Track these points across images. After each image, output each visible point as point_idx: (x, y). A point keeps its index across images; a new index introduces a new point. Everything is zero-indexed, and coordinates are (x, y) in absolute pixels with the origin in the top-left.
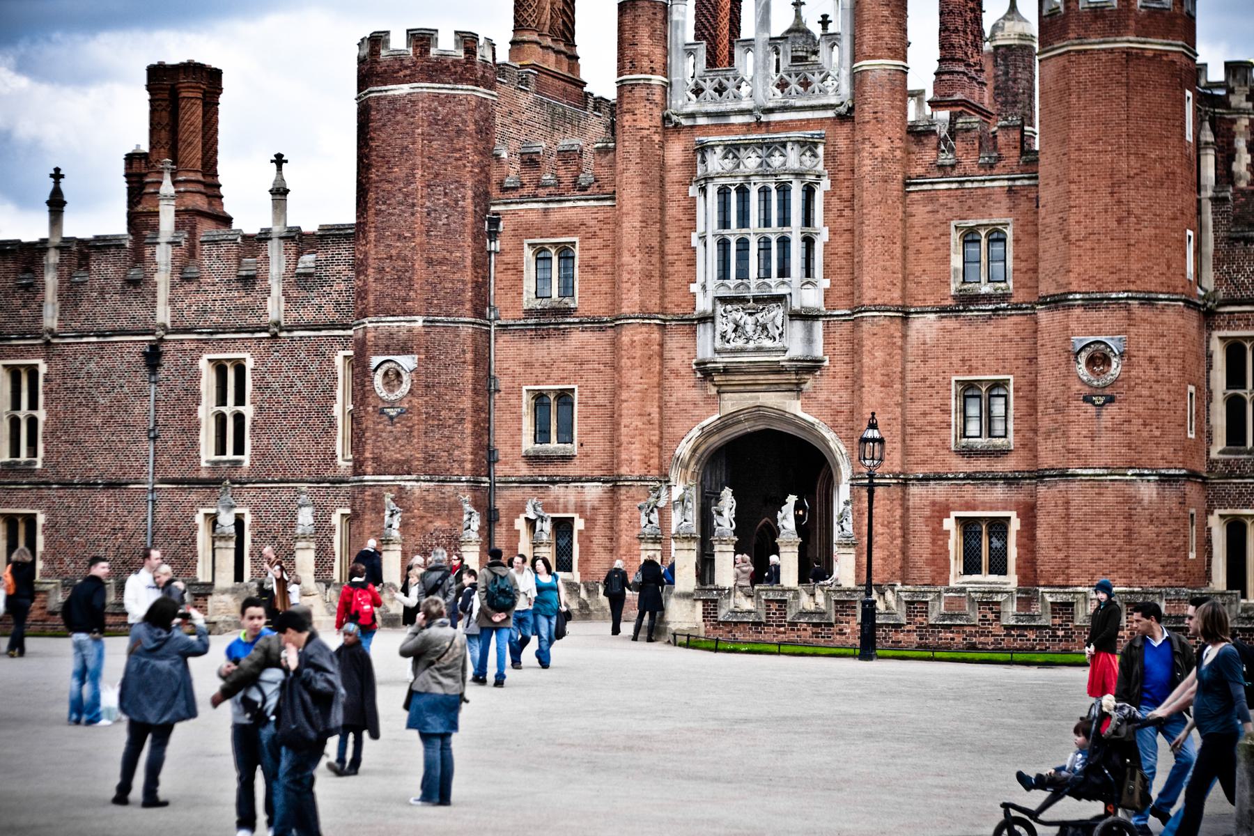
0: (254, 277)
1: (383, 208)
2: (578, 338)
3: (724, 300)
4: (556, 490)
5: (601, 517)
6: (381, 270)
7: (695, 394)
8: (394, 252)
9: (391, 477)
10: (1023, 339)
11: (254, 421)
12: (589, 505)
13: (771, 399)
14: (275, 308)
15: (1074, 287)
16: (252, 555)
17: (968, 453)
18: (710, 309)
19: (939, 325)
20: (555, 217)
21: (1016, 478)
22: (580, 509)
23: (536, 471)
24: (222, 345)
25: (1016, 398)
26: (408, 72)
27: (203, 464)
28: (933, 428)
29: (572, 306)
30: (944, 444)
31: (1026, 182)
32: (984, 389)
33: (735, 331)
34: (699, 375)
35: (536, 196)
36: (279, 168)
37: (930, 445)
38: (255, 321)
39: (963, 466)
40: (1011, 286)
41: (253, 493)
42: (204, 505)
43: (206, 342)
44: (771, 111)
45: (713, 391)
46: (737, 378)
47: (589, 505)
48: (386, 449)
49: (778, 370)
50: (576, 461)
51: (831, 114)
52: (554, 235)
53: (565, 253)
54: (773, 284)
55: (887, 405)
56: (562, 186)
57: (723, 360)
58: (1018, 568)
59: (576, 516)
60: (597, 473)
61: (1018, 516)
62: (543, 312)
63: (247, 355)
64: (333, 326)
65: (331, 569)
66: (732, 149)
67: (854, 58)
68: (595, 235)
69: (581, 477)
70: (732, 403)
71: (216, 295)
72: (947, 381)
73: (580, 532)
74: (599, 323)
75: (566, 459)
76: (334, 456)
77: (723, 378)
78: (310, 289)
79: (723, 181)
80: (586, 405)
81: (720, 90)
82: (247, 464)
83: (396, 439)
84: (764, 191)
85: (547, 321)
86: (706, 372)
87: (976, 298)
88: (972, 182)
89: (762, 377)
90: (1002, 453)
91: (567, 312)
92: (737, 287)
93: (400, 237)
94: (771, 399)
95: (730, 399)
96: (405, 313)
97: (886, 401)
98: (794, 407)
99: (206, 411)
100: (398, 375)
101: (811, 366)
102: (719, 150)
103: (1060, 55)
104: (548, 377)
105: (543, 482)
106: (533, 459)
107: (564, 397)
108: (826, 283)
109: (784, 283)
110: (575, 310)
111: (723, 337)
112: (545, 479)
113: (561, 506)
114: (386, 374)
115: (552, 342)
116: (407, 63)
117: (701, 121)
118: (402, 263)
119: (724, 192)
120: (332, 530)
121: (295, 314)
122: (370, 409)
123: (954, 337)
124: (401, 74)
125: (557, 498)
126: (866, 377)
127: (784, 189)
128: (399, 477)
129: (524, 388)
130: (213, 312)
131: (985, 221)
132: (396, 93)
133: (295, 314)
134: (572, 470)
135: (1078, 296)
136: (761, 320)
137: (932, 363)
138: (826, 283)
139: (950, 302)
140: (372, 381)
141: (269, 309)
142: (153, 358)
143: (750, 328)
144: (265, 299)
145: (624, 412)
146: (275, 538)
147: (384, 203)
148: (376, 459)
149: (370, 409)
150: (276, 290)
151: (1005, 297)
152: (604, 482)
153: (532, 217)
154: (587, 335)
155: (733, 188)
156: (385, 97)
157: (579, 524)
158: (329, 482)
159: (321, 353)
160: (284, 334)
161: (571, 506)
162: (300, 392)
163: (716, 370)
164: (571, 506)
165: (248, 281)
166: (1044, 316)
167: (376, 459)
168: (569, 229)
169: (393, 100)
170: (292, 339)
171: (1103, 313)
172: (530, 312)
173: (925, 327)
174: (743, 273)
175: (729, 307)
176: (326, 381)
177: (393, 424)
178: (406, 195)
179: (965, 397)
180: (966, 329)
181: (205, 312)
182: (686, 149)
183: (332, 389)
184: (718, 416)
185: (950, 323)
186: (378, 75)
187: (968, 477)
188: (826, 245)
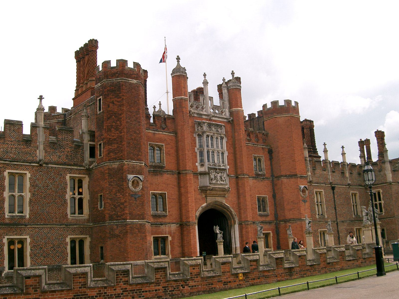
0: (30, 141)
1: (129, 121)
2: (166, 176)
3: (212, 169)
4: (163, 227)
5: (176, 236)
6: (129, 143)
8: (133, 138)
9: (137, 221)
11: (31, 200)
12: (172, 232)
13: (219, 199)
14: (40, 154)
15: (297, 173)
16: (31, 255)
17: (261, 216)
18: (207, 170)
19: (252, 181)
20: (157, 136)
21: (271, 222)
22: (170, 233)
23: (156, 220)
26: (136, 76)
27: (6, 217)
29: (164, 166)
30: (256, 212)
31: (265, 147)
34: (200, 191)
35: (150, 128)
36: (41, 101)
38: (31, 158)
41: (30, 229)
42: (7, 235)
43: (7, 165)
44: (213, 116)
45: (204, 196)
47: (172, 232)
48: (134, 210)
49: (224, 190)
50: (168, 217)
51: (225, 120)
52: (157, 142)
53: (160, 149)
54: (221, 166)
56: (157, 126)
57: (212, 186)
58: (273, 246)
59: (169, 236)
60: (174, 221)
61: (272, 232)
62: (155, 167)
63: (27, 172)
64: (65, 164)
65: (67, 260)
66: (210, 125)
67: (230, 108)
68: (169, 144)
69: (170, 222)
70: (210, 200)
73: (170, 241)
74: (172, 172)
75: (165, 216)
76: (66, 215)
78: (55, 149)
79: (208, 134)
80: (170, 199)
81: (197, 108)
82: (28, 216)
83: (138, 206)
85: (156, 170)
86: (204, 190)
88: (255, 144)
89: (219, 192)
90: (267, 216)
91: (162, 167)
93: (135, 132)
96: (138, 160)
98: (224, 201)
100: (138, 182)
102: (206, 124)
103: (287, 116)
104: (158, 189)
105: (159, 224)
106: (155, 216)
107: (163, 196)
108: (228, 167)
109: (223, 165)
110: (165, 167)
112: (159, 223)
113: (164, 233)
114: (133, 182)
115: (158, 177)
116: (135, 73)
117: (195, 115)
118: (136, 142)
120: (66, 244)
121: (49, 158)
122: (127, 194)
124: (133, 76)
125: (163, 230)
127: (222, 138)
128: (140, 221)
129: (151, 192)
130: (11, 153)
131: (259, 155)
132: (132, 82)
133: (49, 158)
134: (167, 220)
135: (299, 175)
138: (228, 167)
140: (128, 184)
141: (38, 154)
143: (219, 178)
144: (36, 151)
145: (189, 201)
146: (41, 248)
147: (129, 119)
148: (130, 213)
149: (127, 194)
150: (41, 147)
151: (264, 175)
152: (177, 224)
153: (150, 134)
154: (168, 176)
155: (210, 136)
156: (128, 82)
157: (170, 238)
158: (66, 225)
159: (61, 174)
160: (44, 165)
161: (167, 233)
162: (51, 189)
163: (209, 189)
164: (167, 233)
166: (285, 180)
167: (130, 213)
168: (161, 141)
169: (131, 84)
170: (48, 168)
171: (303, 180)
176: (62, 185)
177: (136, 201)
178: (137, 118)
181: (7, 152)
182: (192, 123)
183: (65, 188)
184: (205, 204)
185: (255, 181)
186: (125, 74)
187: (262, 222)
188: (227, 156)
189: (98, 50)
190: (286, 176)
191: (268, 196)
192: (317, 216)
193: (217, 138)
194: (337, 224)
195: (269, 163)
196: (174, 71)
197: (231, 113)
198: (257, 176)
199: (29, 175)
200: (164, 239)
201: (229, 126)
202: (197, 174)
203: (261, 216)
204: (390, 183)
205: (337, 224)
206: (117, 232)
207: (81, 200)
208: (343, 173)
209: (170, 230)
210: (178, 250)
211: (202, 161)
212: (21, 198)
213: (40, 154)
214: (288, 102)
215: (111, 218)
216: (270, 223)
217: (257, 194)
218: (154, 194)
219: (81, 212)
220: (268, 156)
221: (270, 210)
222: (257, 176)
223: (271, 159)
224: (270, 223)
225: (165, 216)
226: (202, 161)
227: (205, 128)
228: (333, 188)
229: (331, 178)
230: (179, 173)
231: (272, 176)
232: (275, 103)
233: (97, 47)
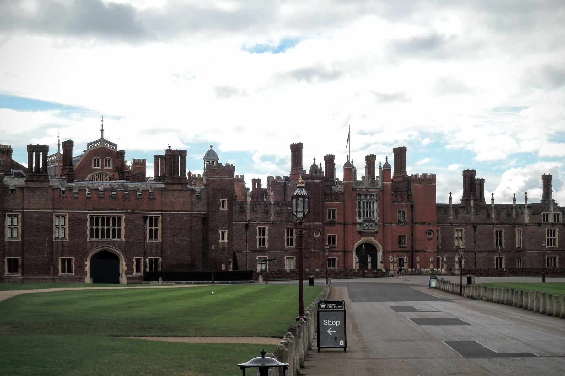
2: (337, 226)
4: (334, 253)
7: (357, 237)
17: (400, 247)
24: (261, 225)
39: (400, 249)
49: (372, 233)
66: (366, 195)
67: (383, 181)
71: (260, 215)
75: (335, 247)
84: (370, 203)
86: (360, 233)
87: (402, 222)
94: (369, 237)
99: (258, 237)
101: (377, 232)
119: (364, 203)
127: (374, 202)
142: (247, 226)
150: (273, 215)
157: (337, 259)
165: (267, 212)
166: (417, 226)
172: (328, 221)
174: (367, 216)
183: (284, 234)
187: (401, 251)
189: (303, 149)
190: (418, 223)
191: (407, 236)
192: (455, 247)
193: (370, 203)
194: (475, 253)
195: (410, 213)
196: (346, 165)
197: (383, 184)
198: (400, 223)
199: (267, 228)
200: (334, 259)
201: (381, 193)
202: (355, 224)
203: (400, 247)
204: (526, 225)
205: (475, 253)
206: (307, 256)
207: (292, 239)
208: (489, 215)
209: (338, 255)
210: (342, 265)
211: (360, 216)
212: (264, 239)
213: (272, 218)
214: (425, 175)
215: (305, 249)
216: (407, 252)
218: (329, 237)
219: (292, 244)
220: (410, 209)
222: (400, 223)
223: (412, 211)
224: (407, 252)
225: (335, 247)
226: (360, 216)
227: (363, 197)
228: (475, 227)
229: (473, 219)
230: (344, 225)
231: (412, 222)
232: (416, 175)
233: (302, 147)
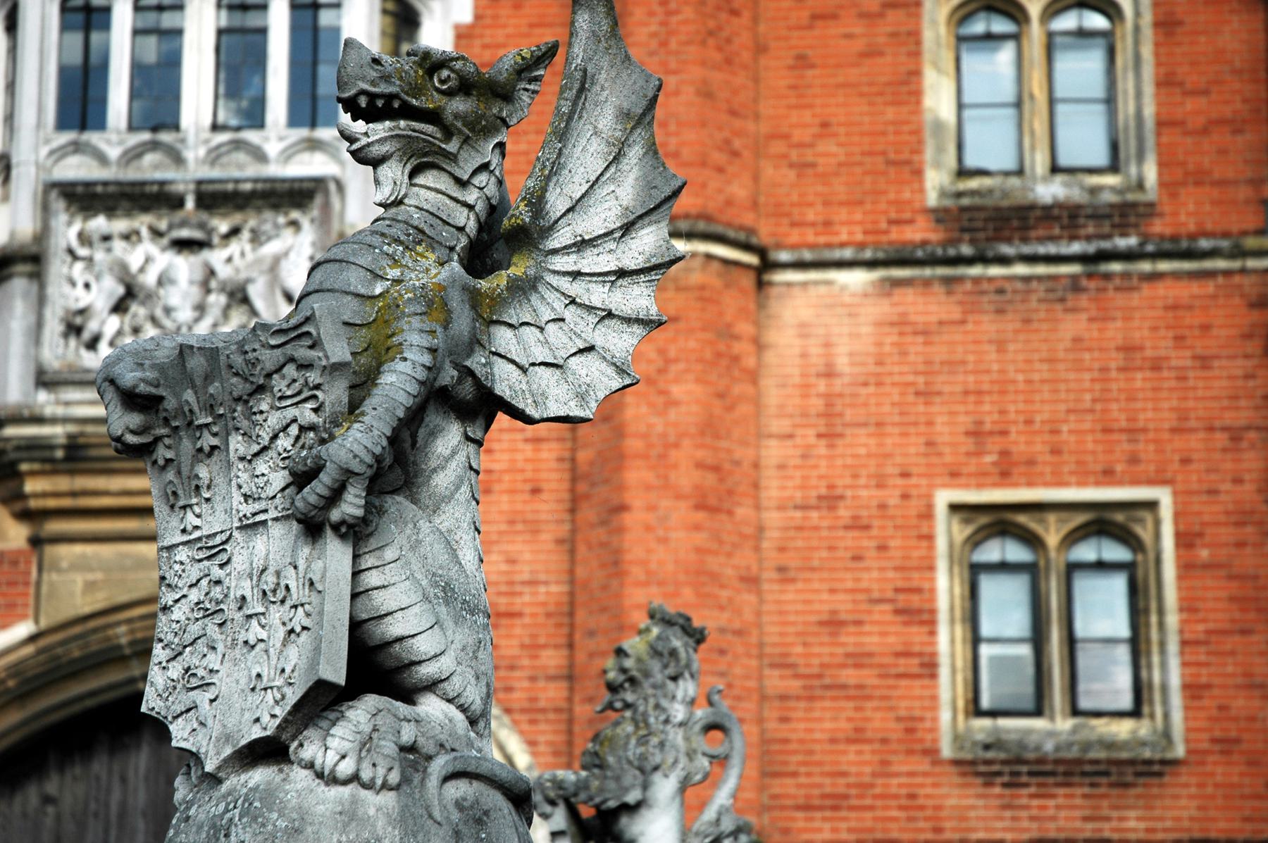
3: (84, 198)
10: (1204, 362)
25: (1186, 568)
28: (868, 677)
32: (1052, 539)
33: (119, 307)
37: (858, 737)
40: (1151, 173)
46: (117, 483)
55: (714, 577)
72: (915, 506)
77: (63, 483)
92: (133, 155)
95: (80, 565)
97: (713, 563)
111: (73, 329)
123: (939, 352)
126: (636, 475)
136: (224, 272)
137: (860, 442)
139: (919, 232)
151: (1126, 214)
173: (829, 315)
175: (99, 223)
179: (976, 570)
180: (988, 325)
217: (954, 476)
221: (1192, 690)
